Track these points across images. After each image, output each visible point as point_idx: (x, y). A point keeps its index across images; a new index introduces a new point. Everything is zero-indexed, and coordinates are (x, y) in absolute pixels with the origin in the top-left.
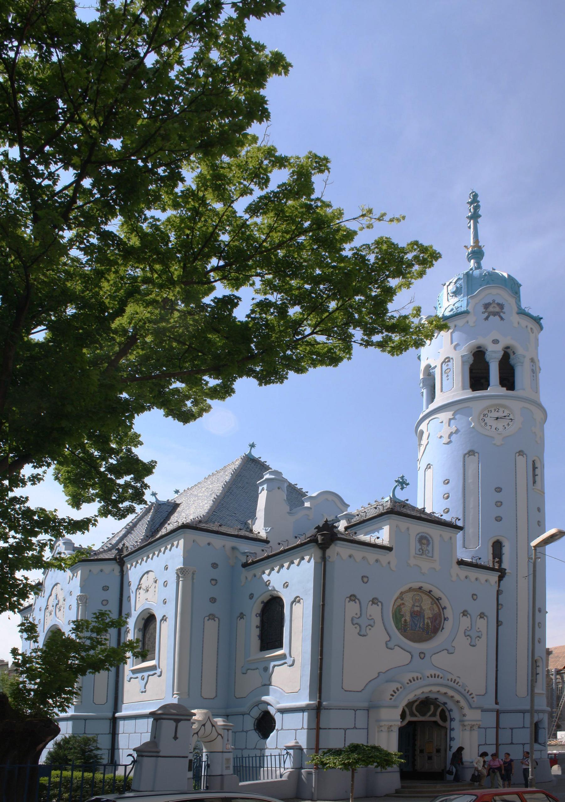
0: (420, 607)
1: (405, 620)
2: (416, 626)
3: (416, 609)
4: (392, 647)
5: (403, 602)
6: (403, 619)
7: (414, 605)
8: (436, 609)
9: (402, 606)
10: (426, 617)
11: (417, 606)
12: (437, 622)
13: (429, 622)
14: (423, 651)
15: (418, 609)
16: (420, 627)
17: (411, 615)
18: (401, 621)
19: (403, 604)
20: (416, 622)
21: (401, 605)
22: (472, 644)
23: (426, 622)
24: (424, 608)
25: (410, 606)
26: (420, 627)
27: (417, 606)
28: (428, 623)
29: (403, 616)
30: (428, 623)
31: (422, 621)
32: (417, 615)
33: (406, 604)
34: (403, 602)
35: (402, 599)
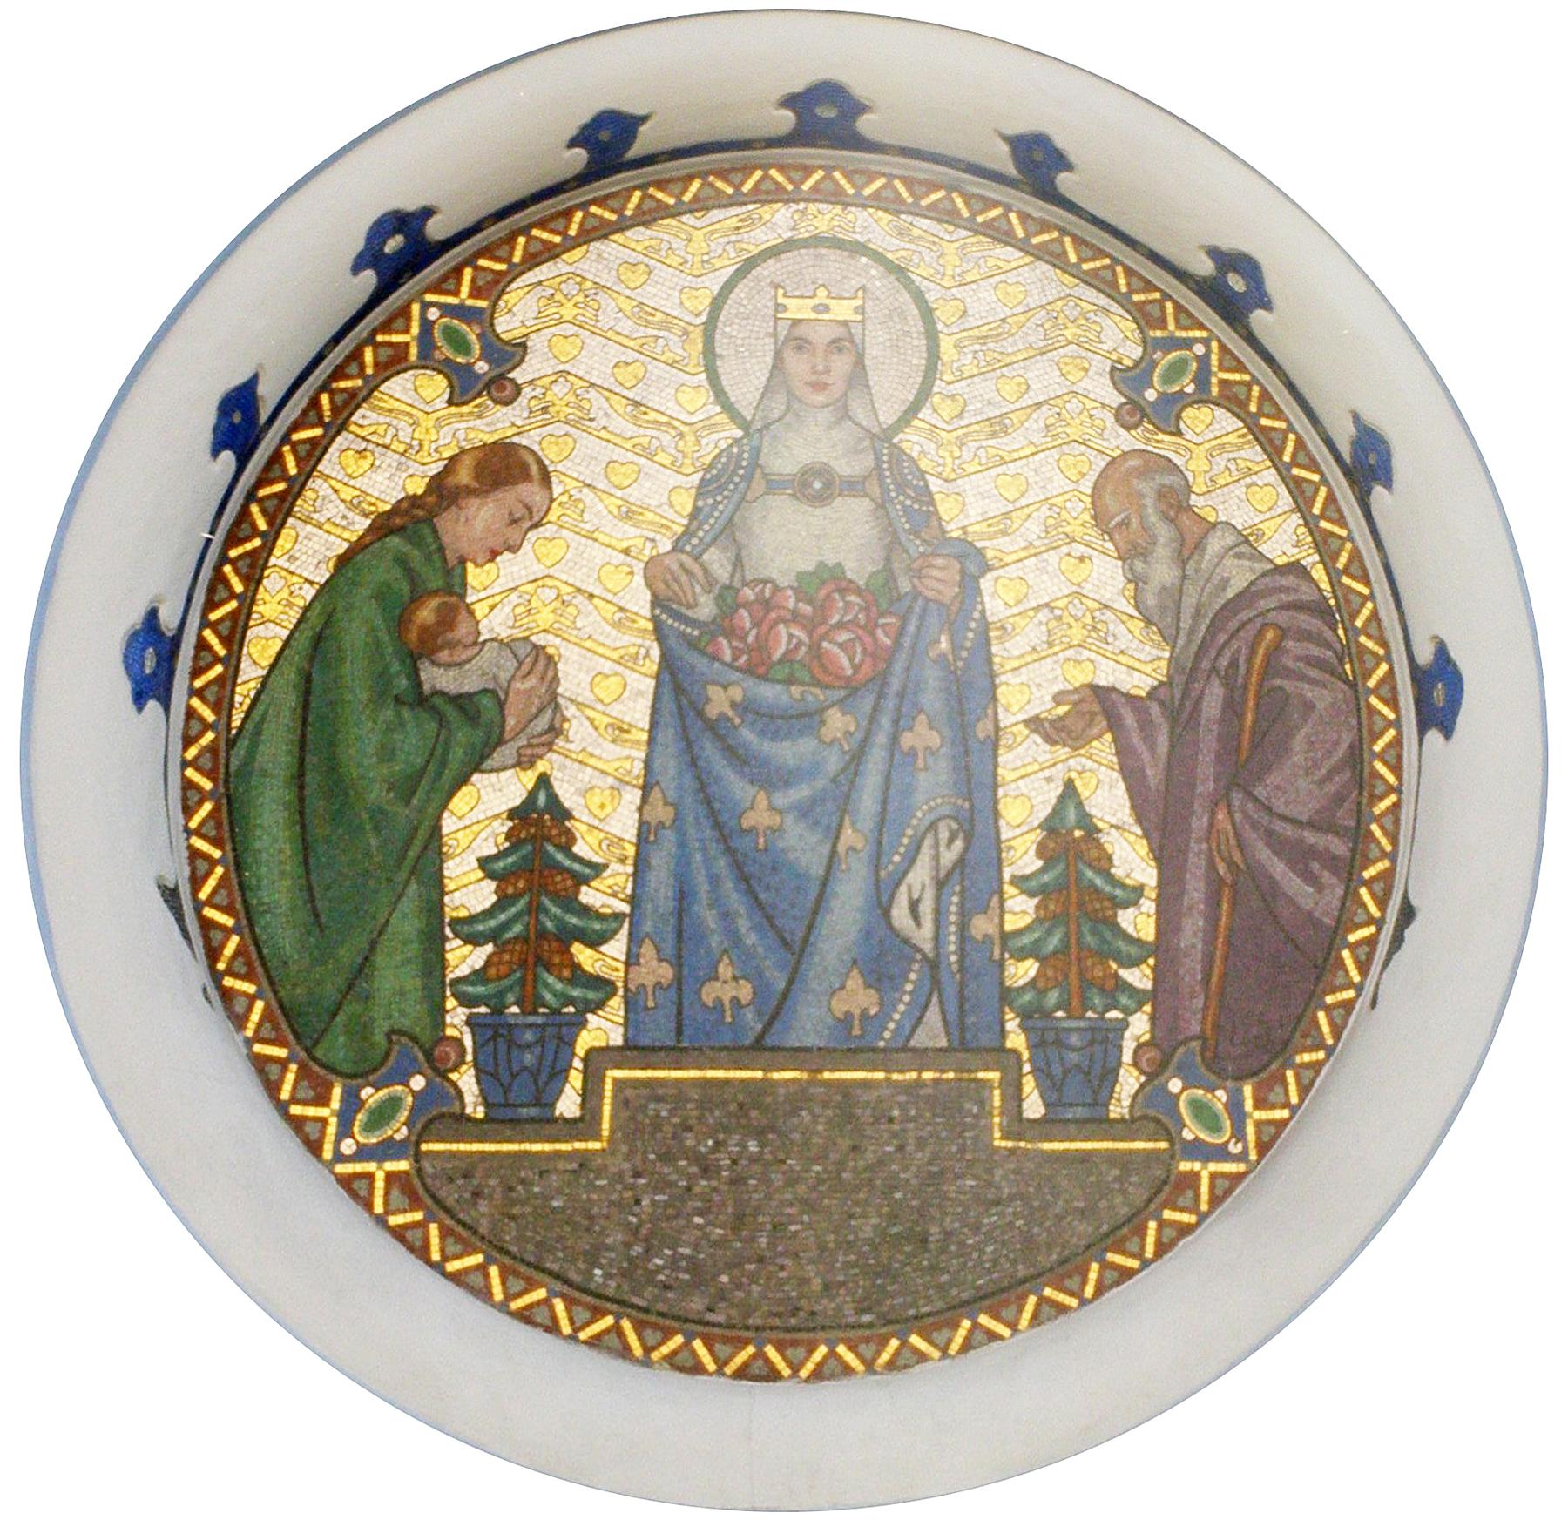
0: (900, 492)
3: (793, 542)
5: (490, 424)
7: (728, 487)
8: (1252, 507)
9: (479, 518)
11: (815, 486)
12: (1296, 786)
13: (1108, 801)
17: (677, 688)
18: (425, 856)
19: (503, 466)
20: (803, 847)
24: (964, 508)
25: (668, 496)
26: (882, 957)
27: (815, 486)
28: (1071, 838)
29: (475, 729)
30: (1071, 838)
33: (572, 459)
34: (490, 424)
35: (489, 374)
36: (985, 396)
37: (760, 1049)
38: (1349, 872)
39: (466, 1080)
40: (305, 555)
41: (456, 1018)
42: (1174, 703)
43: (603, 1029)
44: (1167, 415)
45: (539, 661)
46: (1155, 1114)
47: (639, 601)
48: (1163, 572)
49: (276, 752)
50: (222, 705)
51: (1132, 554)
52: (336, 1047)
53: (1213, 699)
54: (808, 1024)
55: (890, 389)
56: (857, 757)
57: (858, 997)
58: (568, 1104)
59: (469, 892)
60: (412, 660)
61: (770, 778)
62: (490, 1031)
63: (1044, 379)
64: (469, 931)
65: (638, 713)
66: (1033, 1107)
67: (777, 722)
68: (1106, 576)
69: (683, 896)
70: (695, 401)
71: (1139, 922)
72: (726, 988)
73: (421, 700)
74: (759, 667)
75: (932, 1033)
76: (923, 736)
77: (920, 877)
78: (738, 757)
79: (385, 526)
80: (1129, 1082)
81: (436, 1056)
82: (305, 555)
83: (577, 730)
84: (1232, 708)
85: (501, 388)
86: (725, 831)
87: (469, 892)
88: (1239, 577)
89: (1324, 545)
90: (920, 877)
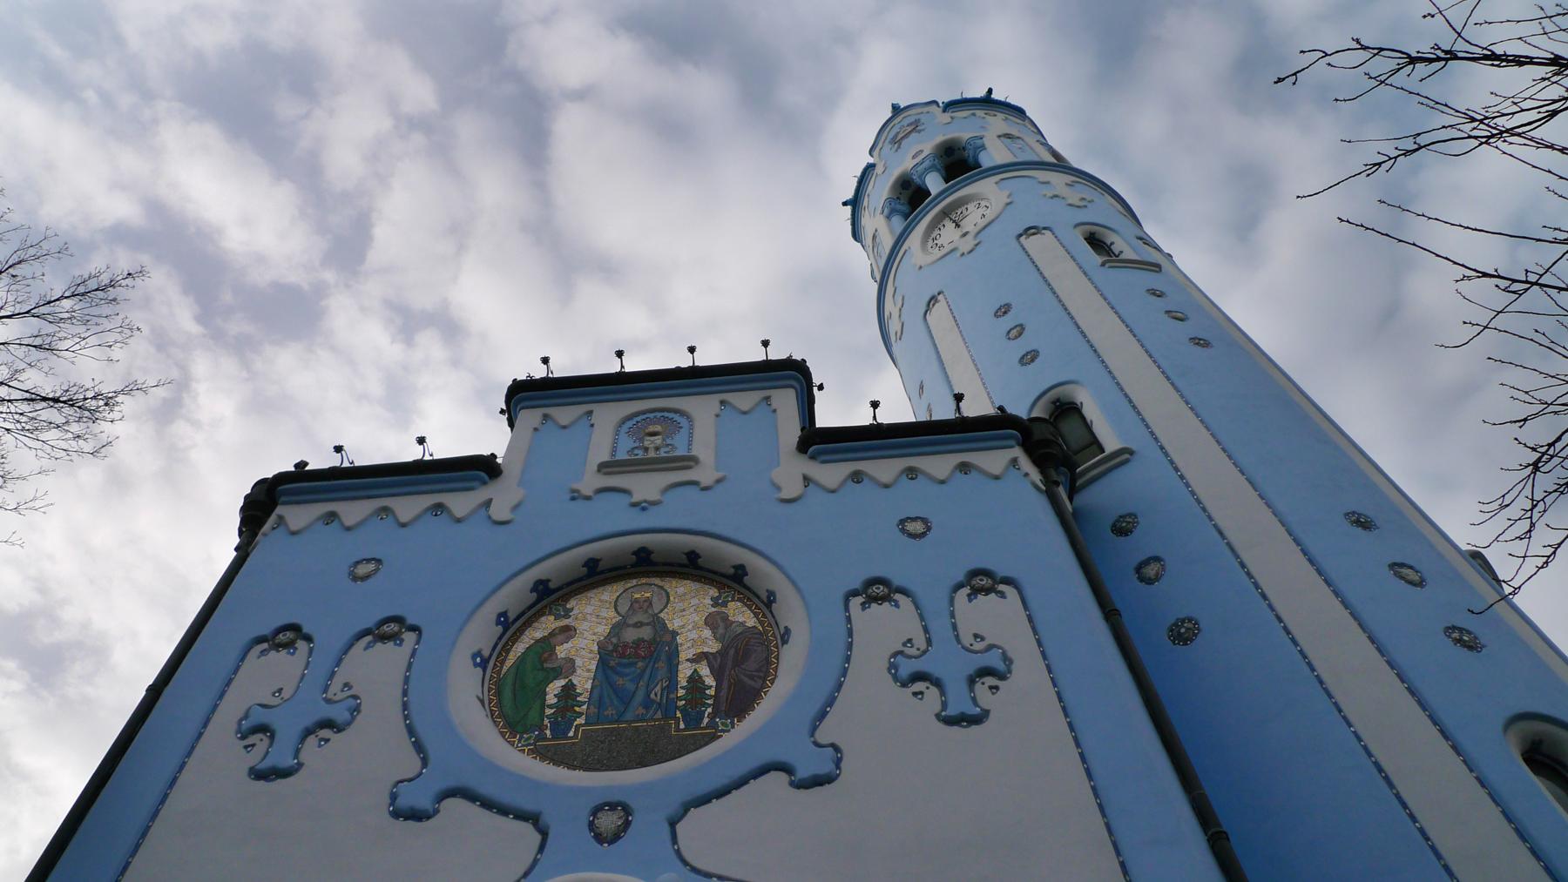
0: (658, 624)
1: (569, 692)
2: (626, 699)
3: (630, 635)
4: (425, 803)
6: (555, 687)
7: (617, 629)
9: (560, 638)
10: (685, 653)
11: (638, 625)
12: (752, 665)
13: (704, 671)
14: (616, 798)
15: (646, 633)
16: (648, 703)
17: (603, 663)
20: (631, 686)
21: (552, 634)
22: (952, 711)
23: (685, 671)
24: (674, 624)
26: (648, 703)
28: (695, 680)
29: (557, 673)
30: (695, 680)
31: (662, 672)
32: (637, 656)
33: (582, 626)
36: (680, 606)
37: (617, 721)
38: (764, 680)
39: (548, 732)
40: (520, 648)
41: (546, 721)
42: (722, 653)
43: (581, 721)
44: (725, 604)
45: (572, 661)
46: (715, 726)
47: (595, 648)
48: (721, 631)
49: (509, 681)
50: (499, 672)
51: (714, 629)
52: (519, 728)
53: (732, 652)
54: (629, 716)
55: (657, 607)
56: (644, 671)
57: (641, 710)
58: (571, 734)
59: (551, 699)
60: (542, 663)
61: (622, 675)
62: (555, 726)
63: (695, 601)
64: (550, 707)
65: (594, 667)
66: (682, 726)
67: (625, 666)
68: (707, 633)
69: (601, 698)
70: (612, 613)
71: (712, 692)
72: (609, 712)
73: (543, 669)
74: (623, 656)
75: (659, 715)
76: (660, 664)
77: (658, 688)
78: (617, 673)
79: (537, 641)
80: (706, 720)
81: (541, 728)
82: (520, 648)
83: (579, 671)
84: (737, 652)
85: (567, 616)
86: (611, 685)
87: (551, 699)
88: (740, 630)
89: (762, 623)
90: (658, 688)
